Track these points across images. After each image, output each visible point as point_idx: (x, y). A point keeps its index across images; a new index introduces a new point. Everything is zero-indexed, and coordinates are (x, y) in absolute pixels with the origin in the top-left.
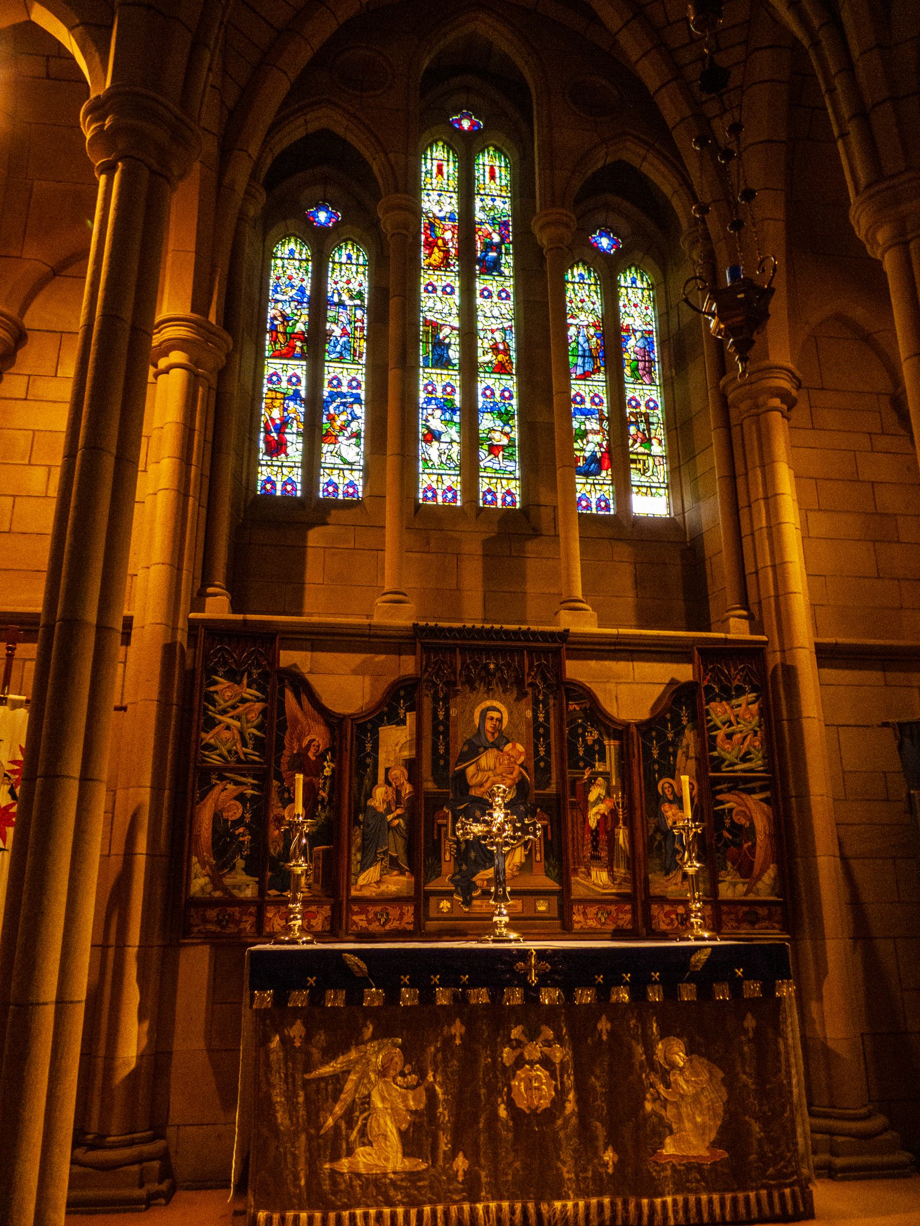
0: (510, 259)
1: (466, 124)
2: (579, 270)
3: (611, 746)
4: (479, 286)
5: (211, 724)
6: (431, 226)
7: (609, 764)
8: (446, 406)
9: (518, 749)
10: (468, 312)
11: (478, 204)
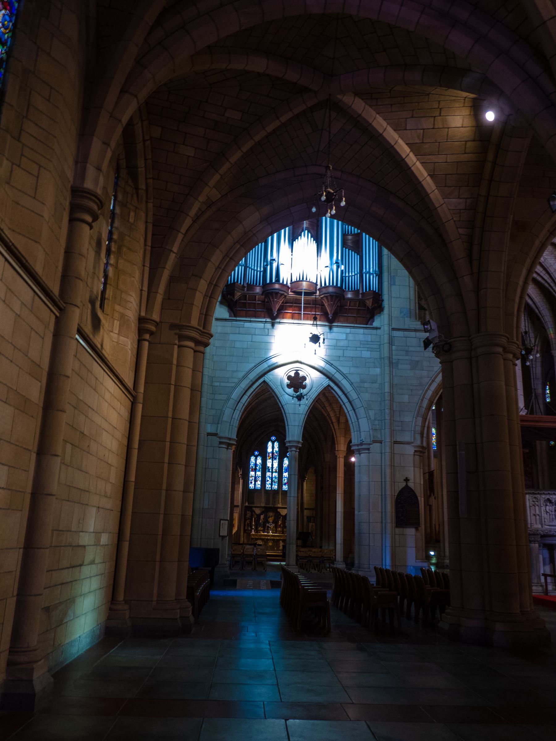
0: (278, 458)
1: (273, 438)
2: (285, 459)
3: (281, 517)
4: (274, 461)
5: (247, 515)
6: (269, 454)
7: (281, 519)
8: (270, 477)
9: (273, 518)
10: (272, 465)
11: (274, 450)
